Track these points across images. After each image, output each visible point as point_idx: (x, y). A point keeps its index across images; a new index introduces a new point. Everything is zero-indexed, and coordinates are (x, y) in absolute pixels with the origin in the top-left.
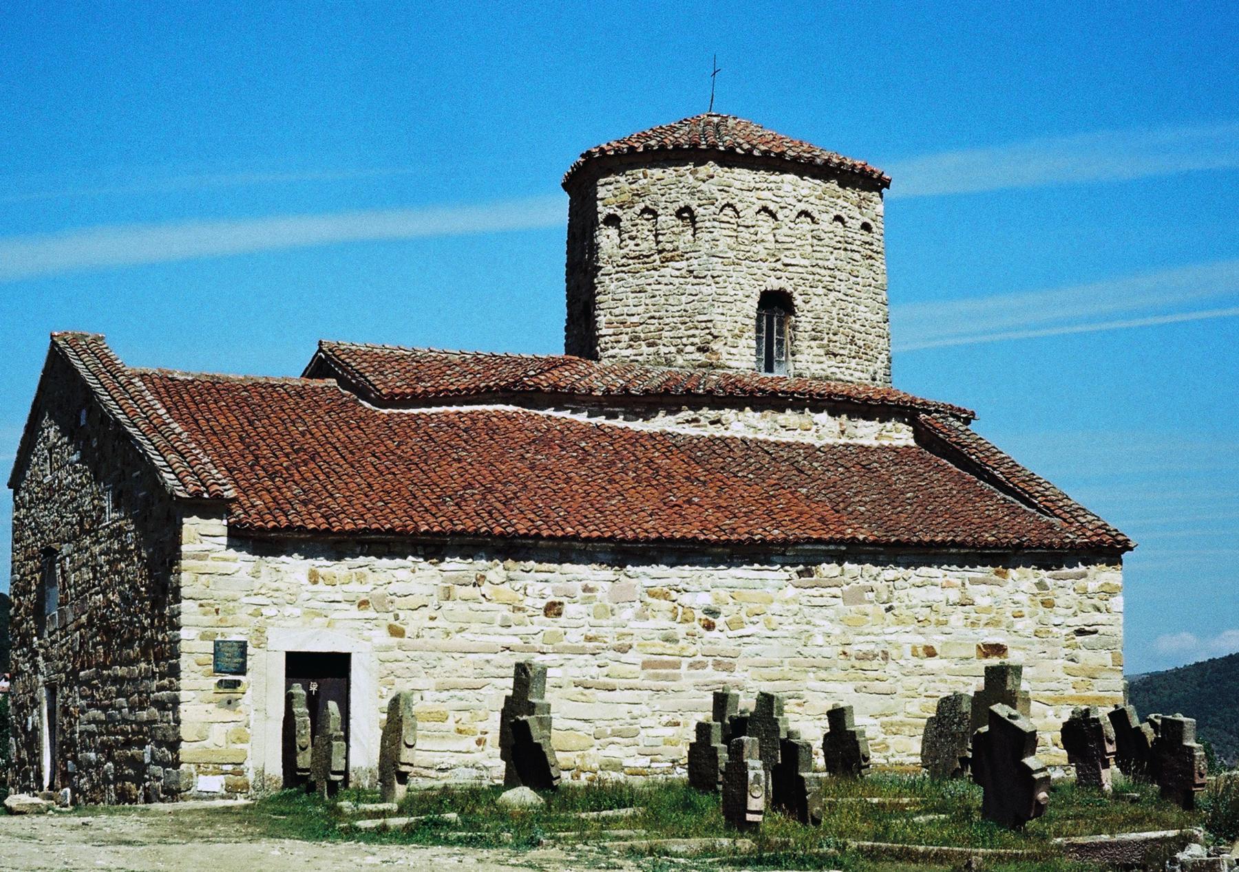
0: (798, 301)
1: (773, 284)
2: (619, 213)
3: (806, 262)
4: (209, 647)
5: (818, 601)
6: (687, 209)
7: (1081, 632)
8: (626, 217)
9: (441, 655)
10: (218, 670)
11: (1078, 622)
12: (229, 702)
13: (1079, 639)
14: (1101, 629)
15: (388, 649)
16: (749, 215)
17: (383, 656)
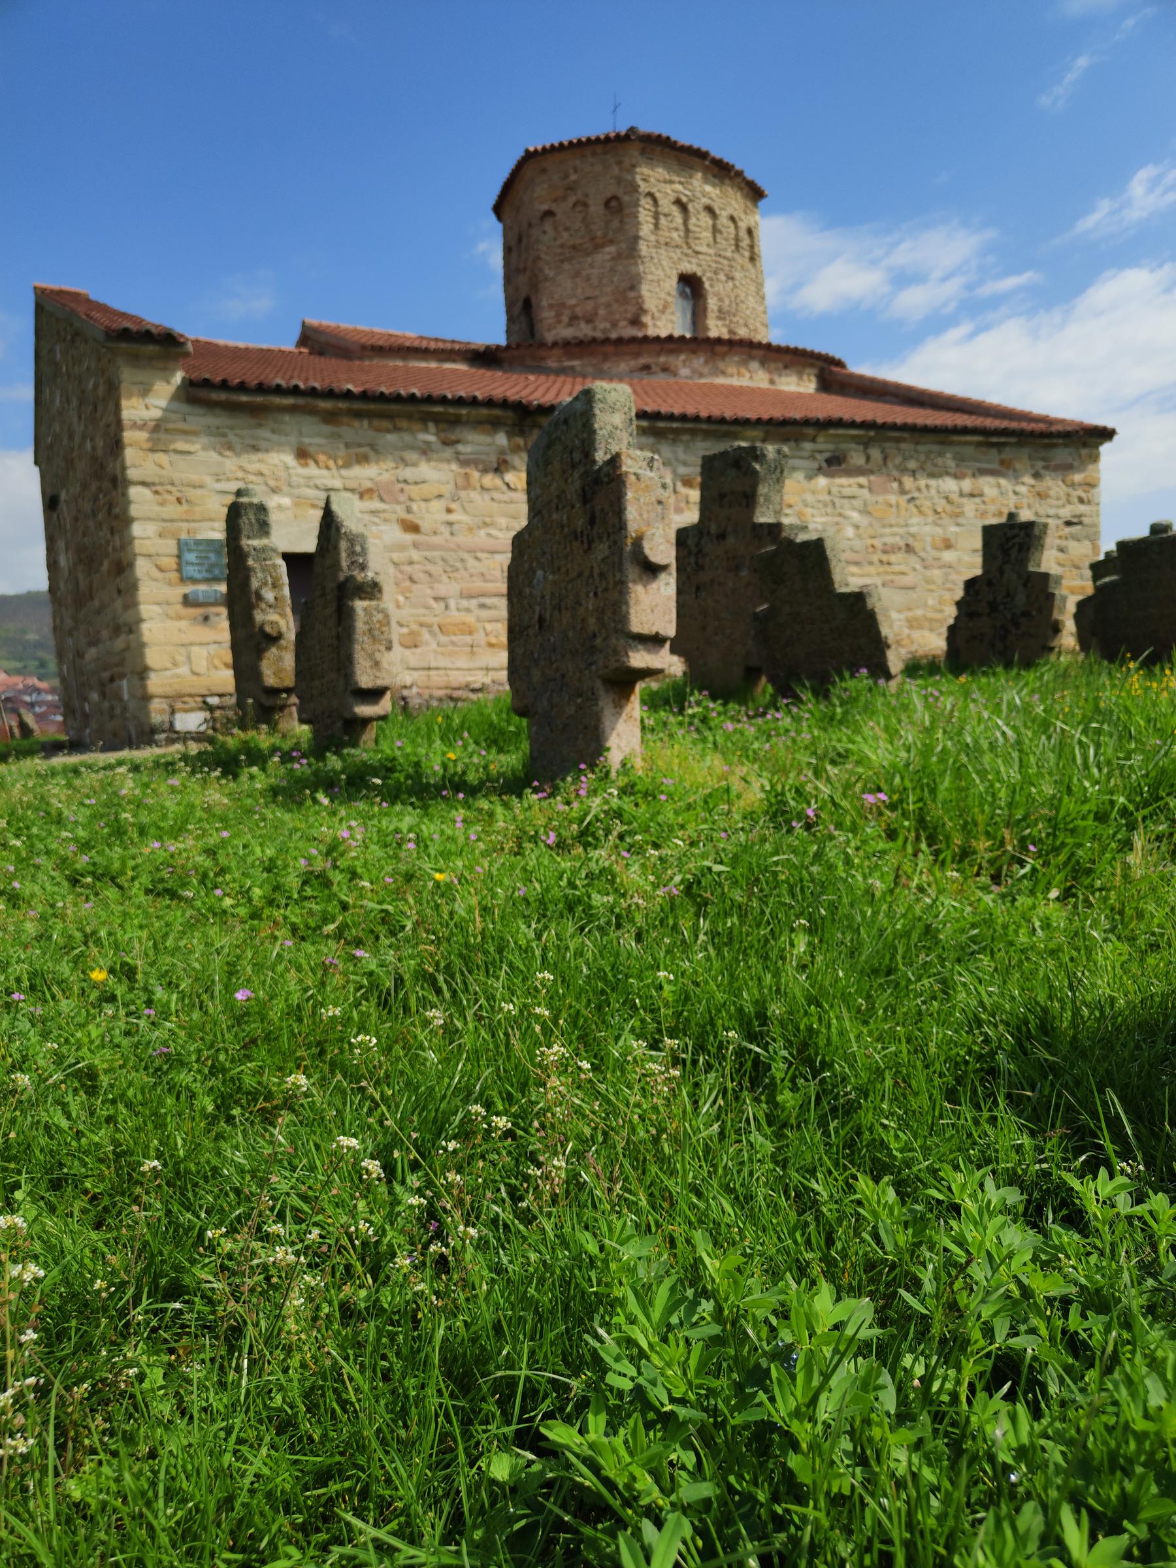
0: (707, 285)
1: (689, 267)
2: (554, 207)
3: (711, 251)
4: (171, 546)
5: (847, 492)
6: (615, 198)
7: (1068, 523)
8: (561, 209)
9: (466, 556)
10: (183, 580)
11: (1066, 512)
12: (206, 618)
13: (1068, 530)
14: (1086, 520)
15: (401, 548)
16: (666, 204)
17: (396, 556)
